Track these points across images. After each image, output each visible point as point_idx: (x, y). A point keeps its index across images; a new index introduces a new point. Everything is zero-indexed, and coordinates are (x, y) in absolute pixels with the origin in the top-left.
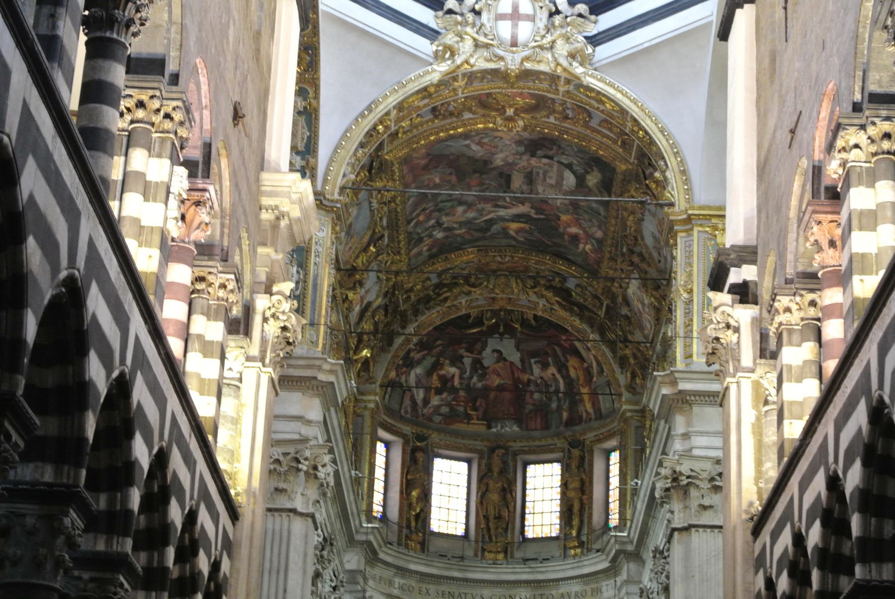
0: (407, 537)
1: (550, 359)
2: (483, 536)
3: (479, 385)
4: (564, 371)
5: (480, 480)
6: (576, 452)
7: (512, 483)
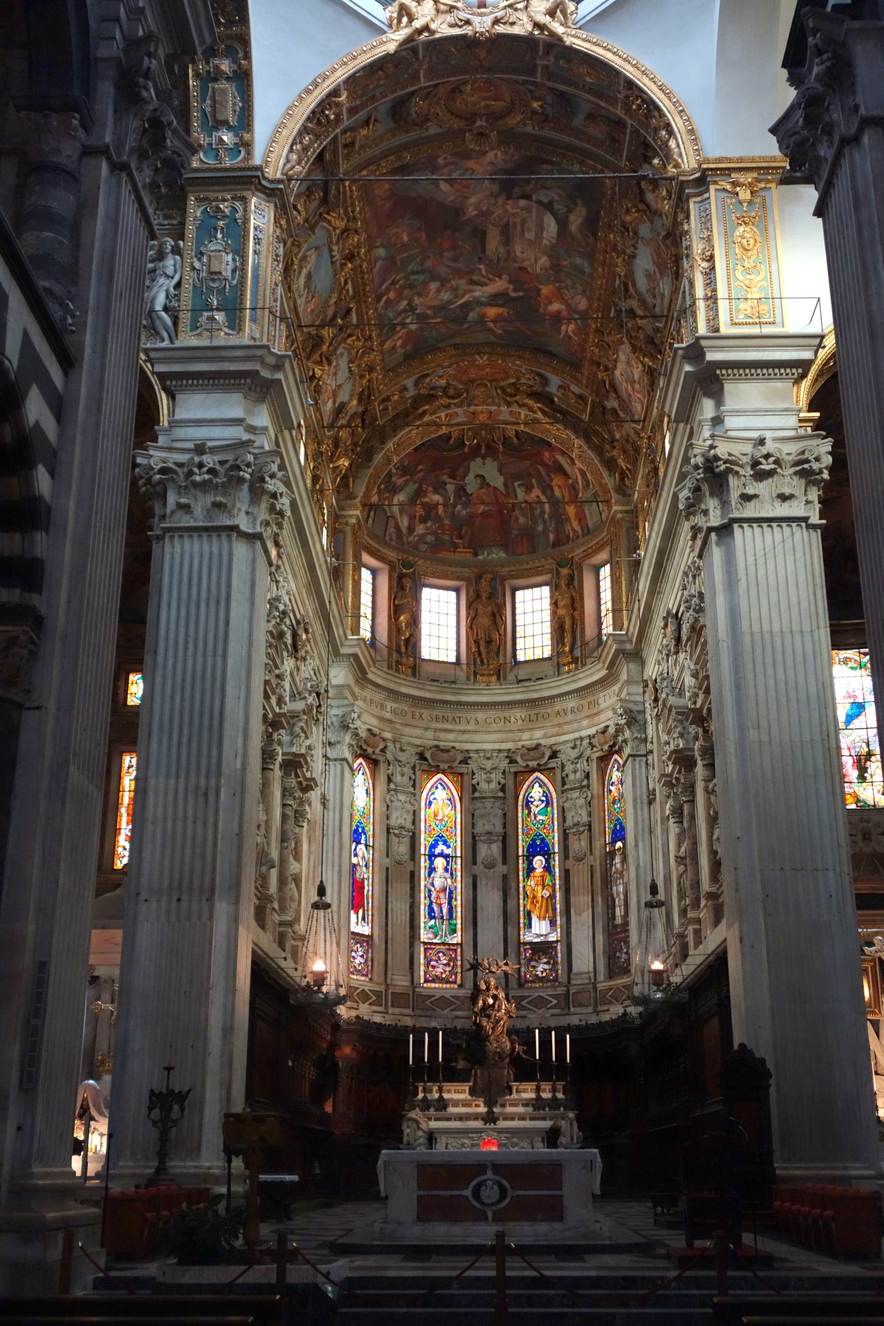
0: (397, 662)
1: (534, 481)
2: (475, 660)
3: (464, 513)
4: (549, 492)
5: (469, 606)
6: (565, 571)
7: (501, 608)
